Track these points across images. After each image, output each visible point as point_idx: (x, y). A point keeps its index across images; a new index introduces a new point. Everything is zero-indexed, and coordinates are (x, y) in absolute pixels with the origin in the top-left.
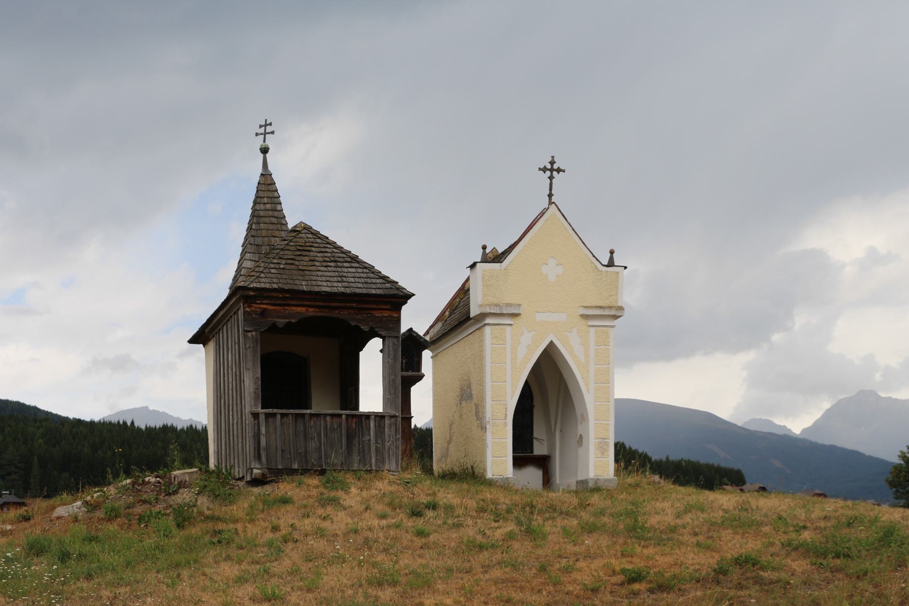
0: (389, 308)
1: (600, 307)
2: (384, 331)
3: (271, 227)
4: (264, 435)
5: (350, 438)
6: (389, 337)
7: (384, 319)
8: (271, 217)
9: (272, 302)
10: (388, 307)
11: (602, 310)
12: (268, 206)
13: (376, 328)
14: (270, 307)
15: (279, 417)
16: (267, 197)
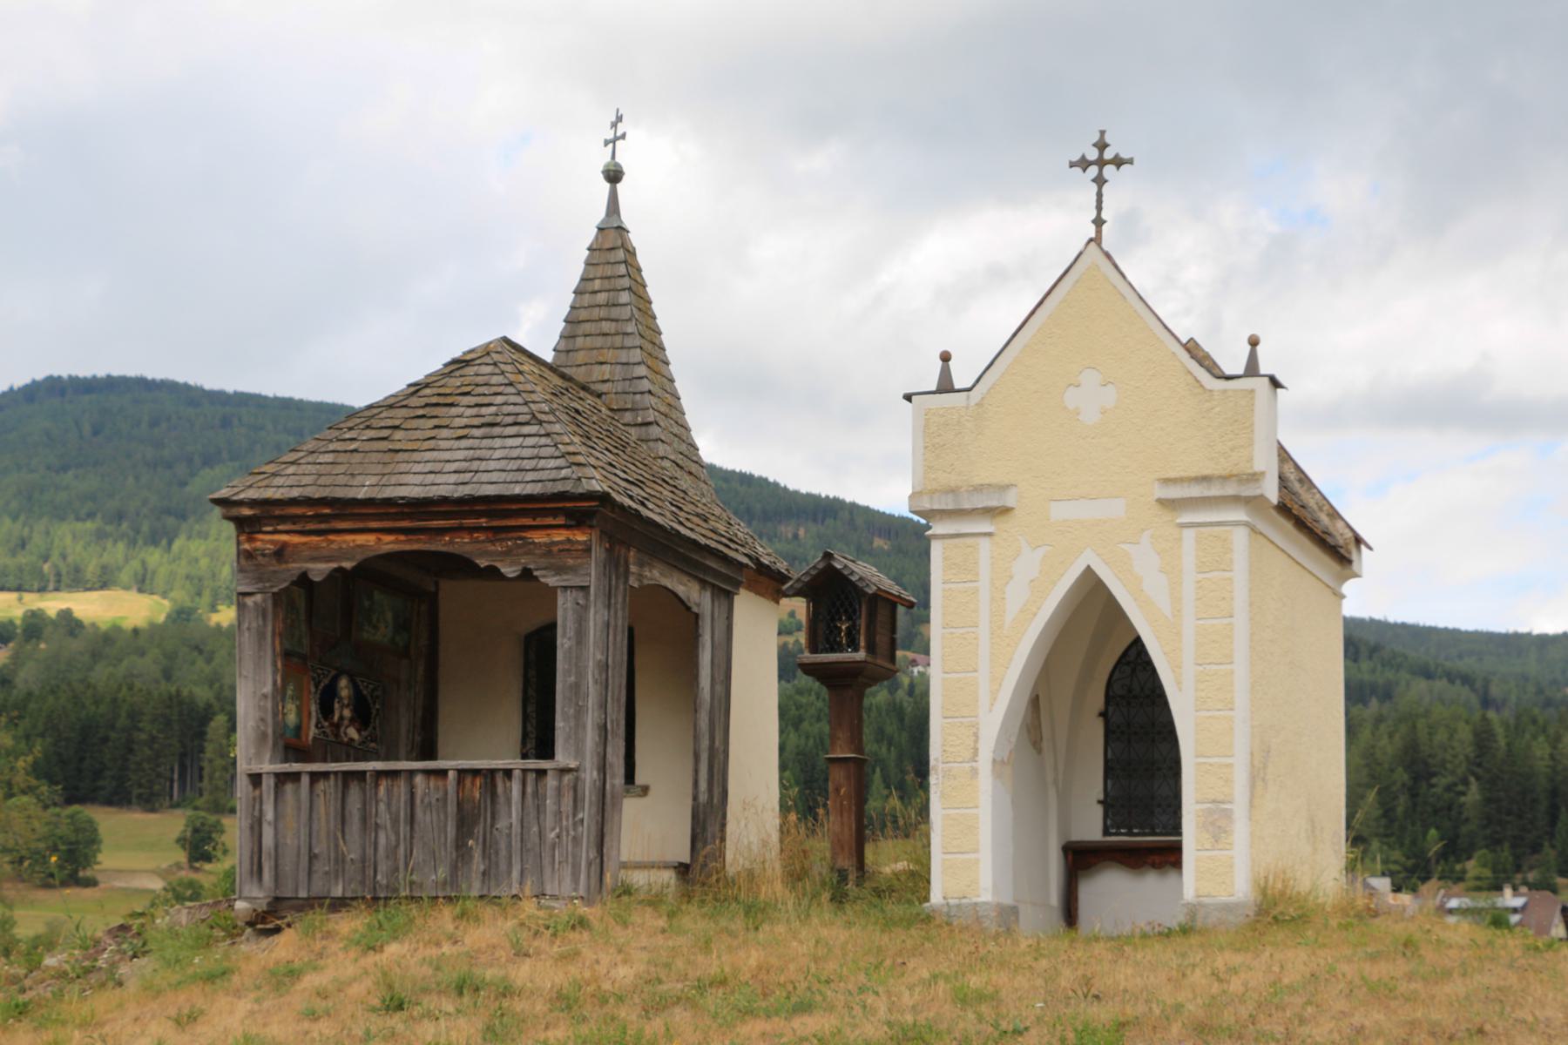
0: (563, 522)
1: (1205, 479)
2: (554, 576)
3: (599, 341)
4: (269, 823)
5: (465, 823)
6: (565, 588)
7: (555, 549)
8: (601, 320)
9: (297, 527)
10: (560, 521)
11: (1205, 484)
12: (602, 298)
13: (537, 570)
14: (296, 539)
15: (305, 780)
16: (601, 278)
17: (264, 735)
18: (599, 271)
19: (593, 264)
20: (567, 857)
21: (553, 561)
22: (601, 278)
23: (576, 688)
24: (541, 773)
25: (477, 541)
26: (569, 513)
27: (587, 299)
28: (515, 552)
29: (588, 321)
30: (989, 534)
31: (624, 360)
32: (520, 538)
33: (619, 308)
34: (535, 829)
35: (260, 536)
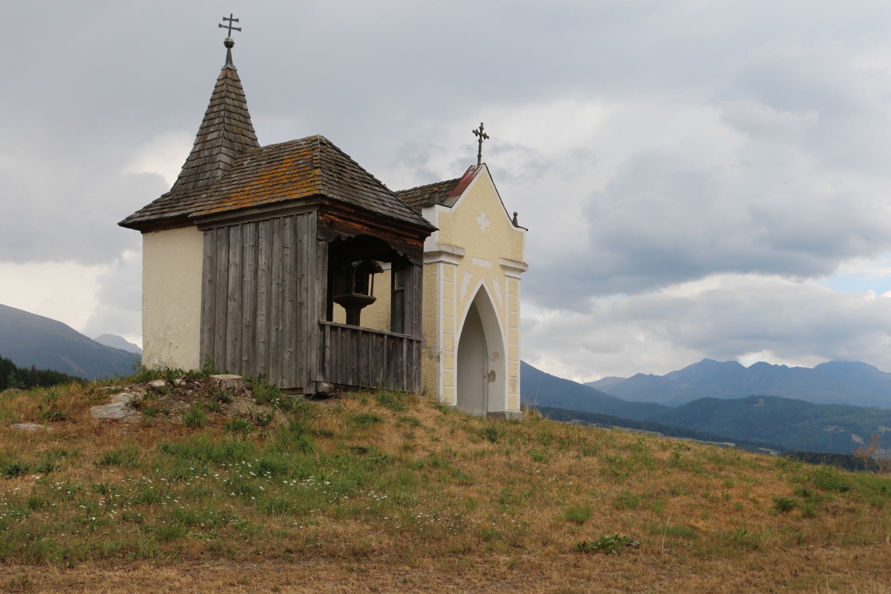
14: (337, 220)
30: (457, 265)
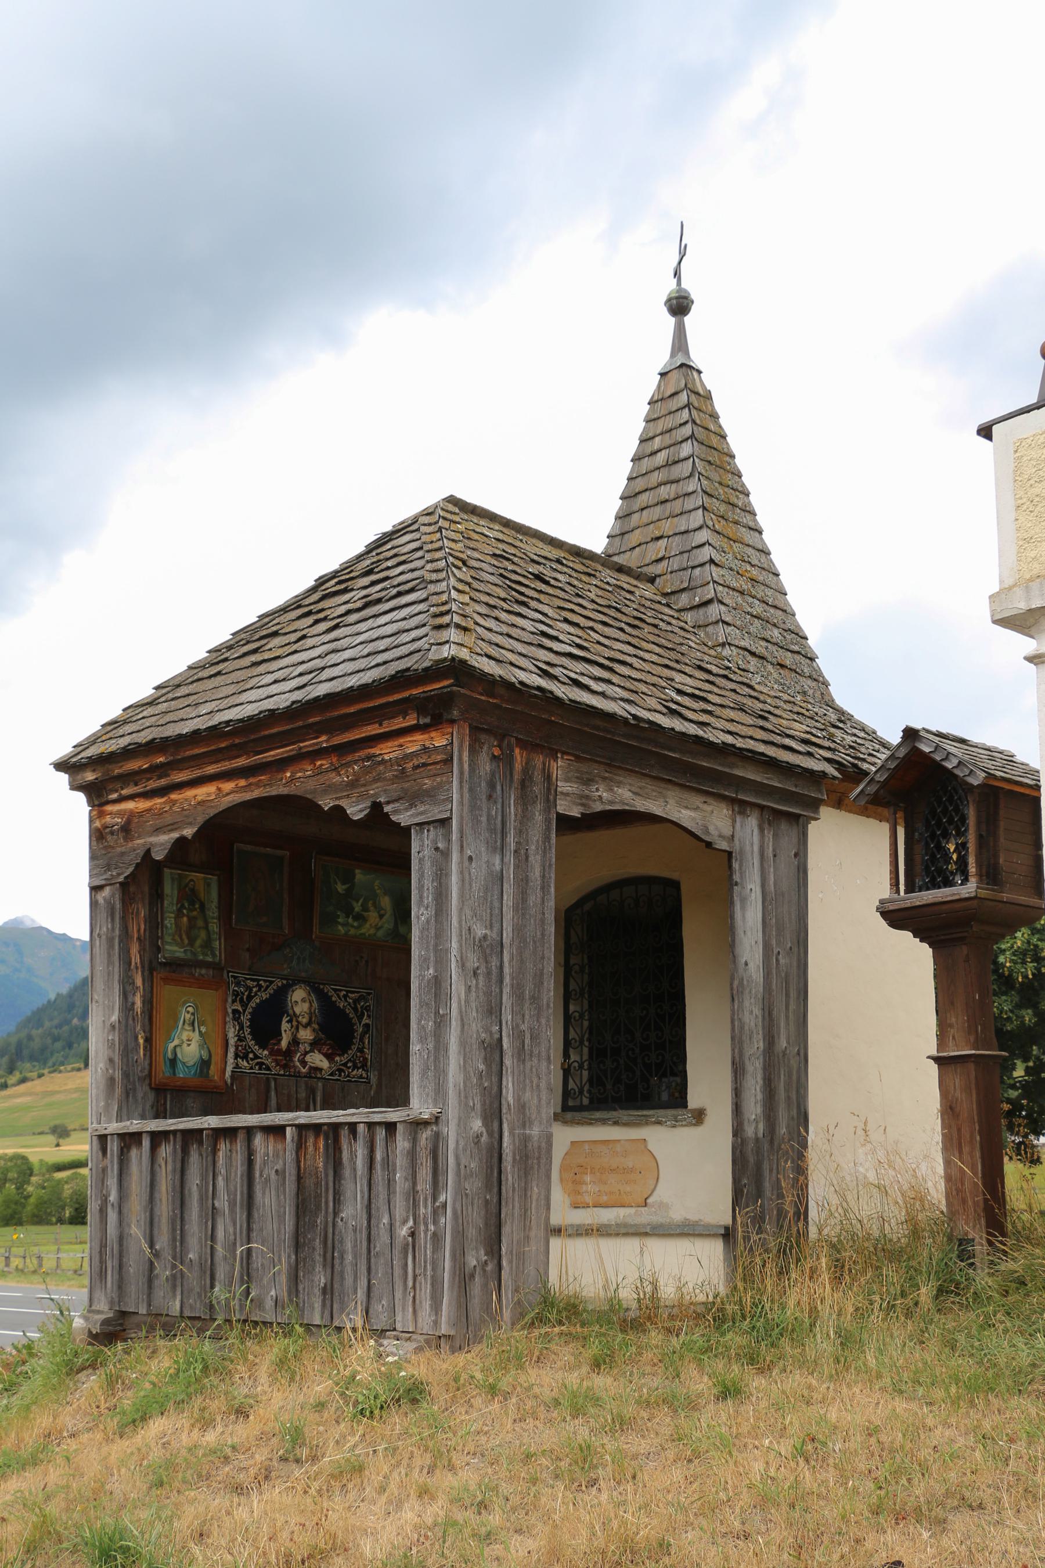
2: (406, 810)
3: (657, 512)
6: (420, 824)
7: (409, 766)
9: (138, 789)
10: (411, 720)
13: (388, 803)
14: (142, 805)
17: (111, 1080)
18: (660, 426)
19: (655, 420)
20: (425, 1266)
21: (406, 785)
22: (662, 434)
23: (438, 985)
24: (391, 1127)
25: (319, 772)
26: (421, 705)
27: (646, 464)
28: (362, 781)
29: (646, 490)
31: (683, 529)
32: (369, 758)
33: (680, 465)
34: (385, 1220)
35: (109, 808)
